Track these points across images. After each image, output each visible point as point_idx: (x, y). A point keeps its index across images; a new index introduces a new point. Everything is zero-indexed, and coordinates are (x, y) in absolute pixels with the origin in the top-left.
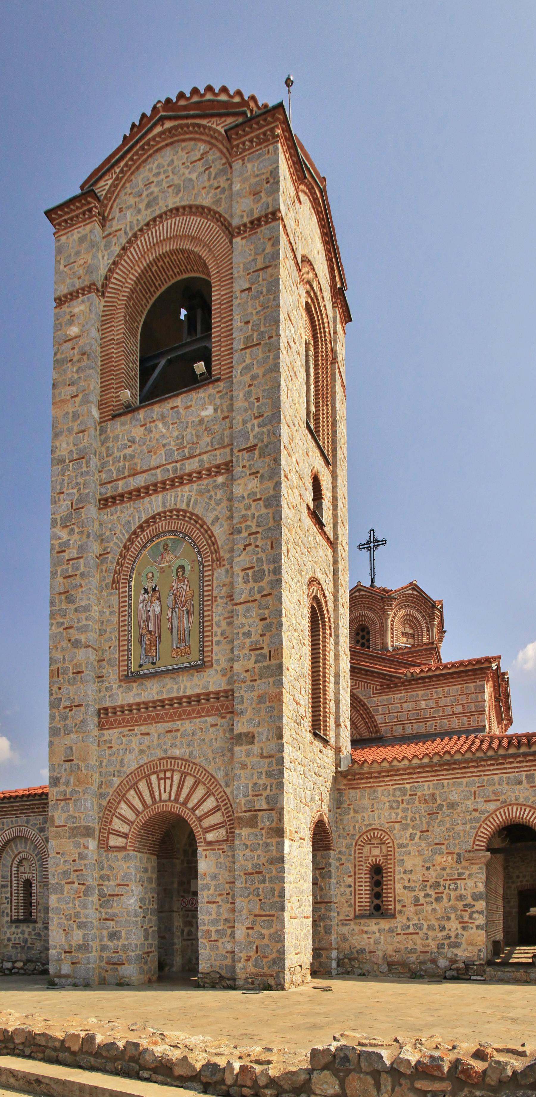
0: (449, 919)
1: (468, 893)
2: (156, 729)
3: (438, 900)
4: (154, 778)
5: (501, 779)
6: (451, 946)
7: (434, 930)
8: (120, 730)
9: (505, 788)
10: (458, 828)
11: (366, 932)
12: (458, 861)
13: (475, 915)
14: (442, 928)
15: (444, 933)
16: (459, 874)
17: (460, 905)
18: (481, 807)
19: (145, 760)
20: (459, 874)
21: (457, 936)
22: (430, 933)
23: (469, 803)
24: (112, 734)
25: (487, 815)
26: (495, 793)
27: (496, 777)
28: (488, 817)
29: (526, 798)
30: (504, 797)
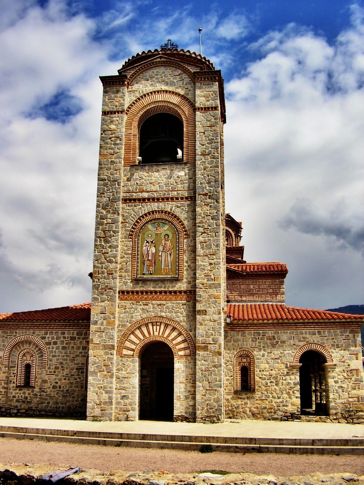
5: (306, 332)
7: (275, 398)
8: (131, 302)
9: (308, 336)
11: (241, 398)
14: (279, 398)
15: (280, 400)
20: (287, 373)
21: (286, 401)
23: (291, 341)
25: (300, 347)
26: (304, 338)
27: (304, 331)
28: (300, 348)
30: (308, 340)
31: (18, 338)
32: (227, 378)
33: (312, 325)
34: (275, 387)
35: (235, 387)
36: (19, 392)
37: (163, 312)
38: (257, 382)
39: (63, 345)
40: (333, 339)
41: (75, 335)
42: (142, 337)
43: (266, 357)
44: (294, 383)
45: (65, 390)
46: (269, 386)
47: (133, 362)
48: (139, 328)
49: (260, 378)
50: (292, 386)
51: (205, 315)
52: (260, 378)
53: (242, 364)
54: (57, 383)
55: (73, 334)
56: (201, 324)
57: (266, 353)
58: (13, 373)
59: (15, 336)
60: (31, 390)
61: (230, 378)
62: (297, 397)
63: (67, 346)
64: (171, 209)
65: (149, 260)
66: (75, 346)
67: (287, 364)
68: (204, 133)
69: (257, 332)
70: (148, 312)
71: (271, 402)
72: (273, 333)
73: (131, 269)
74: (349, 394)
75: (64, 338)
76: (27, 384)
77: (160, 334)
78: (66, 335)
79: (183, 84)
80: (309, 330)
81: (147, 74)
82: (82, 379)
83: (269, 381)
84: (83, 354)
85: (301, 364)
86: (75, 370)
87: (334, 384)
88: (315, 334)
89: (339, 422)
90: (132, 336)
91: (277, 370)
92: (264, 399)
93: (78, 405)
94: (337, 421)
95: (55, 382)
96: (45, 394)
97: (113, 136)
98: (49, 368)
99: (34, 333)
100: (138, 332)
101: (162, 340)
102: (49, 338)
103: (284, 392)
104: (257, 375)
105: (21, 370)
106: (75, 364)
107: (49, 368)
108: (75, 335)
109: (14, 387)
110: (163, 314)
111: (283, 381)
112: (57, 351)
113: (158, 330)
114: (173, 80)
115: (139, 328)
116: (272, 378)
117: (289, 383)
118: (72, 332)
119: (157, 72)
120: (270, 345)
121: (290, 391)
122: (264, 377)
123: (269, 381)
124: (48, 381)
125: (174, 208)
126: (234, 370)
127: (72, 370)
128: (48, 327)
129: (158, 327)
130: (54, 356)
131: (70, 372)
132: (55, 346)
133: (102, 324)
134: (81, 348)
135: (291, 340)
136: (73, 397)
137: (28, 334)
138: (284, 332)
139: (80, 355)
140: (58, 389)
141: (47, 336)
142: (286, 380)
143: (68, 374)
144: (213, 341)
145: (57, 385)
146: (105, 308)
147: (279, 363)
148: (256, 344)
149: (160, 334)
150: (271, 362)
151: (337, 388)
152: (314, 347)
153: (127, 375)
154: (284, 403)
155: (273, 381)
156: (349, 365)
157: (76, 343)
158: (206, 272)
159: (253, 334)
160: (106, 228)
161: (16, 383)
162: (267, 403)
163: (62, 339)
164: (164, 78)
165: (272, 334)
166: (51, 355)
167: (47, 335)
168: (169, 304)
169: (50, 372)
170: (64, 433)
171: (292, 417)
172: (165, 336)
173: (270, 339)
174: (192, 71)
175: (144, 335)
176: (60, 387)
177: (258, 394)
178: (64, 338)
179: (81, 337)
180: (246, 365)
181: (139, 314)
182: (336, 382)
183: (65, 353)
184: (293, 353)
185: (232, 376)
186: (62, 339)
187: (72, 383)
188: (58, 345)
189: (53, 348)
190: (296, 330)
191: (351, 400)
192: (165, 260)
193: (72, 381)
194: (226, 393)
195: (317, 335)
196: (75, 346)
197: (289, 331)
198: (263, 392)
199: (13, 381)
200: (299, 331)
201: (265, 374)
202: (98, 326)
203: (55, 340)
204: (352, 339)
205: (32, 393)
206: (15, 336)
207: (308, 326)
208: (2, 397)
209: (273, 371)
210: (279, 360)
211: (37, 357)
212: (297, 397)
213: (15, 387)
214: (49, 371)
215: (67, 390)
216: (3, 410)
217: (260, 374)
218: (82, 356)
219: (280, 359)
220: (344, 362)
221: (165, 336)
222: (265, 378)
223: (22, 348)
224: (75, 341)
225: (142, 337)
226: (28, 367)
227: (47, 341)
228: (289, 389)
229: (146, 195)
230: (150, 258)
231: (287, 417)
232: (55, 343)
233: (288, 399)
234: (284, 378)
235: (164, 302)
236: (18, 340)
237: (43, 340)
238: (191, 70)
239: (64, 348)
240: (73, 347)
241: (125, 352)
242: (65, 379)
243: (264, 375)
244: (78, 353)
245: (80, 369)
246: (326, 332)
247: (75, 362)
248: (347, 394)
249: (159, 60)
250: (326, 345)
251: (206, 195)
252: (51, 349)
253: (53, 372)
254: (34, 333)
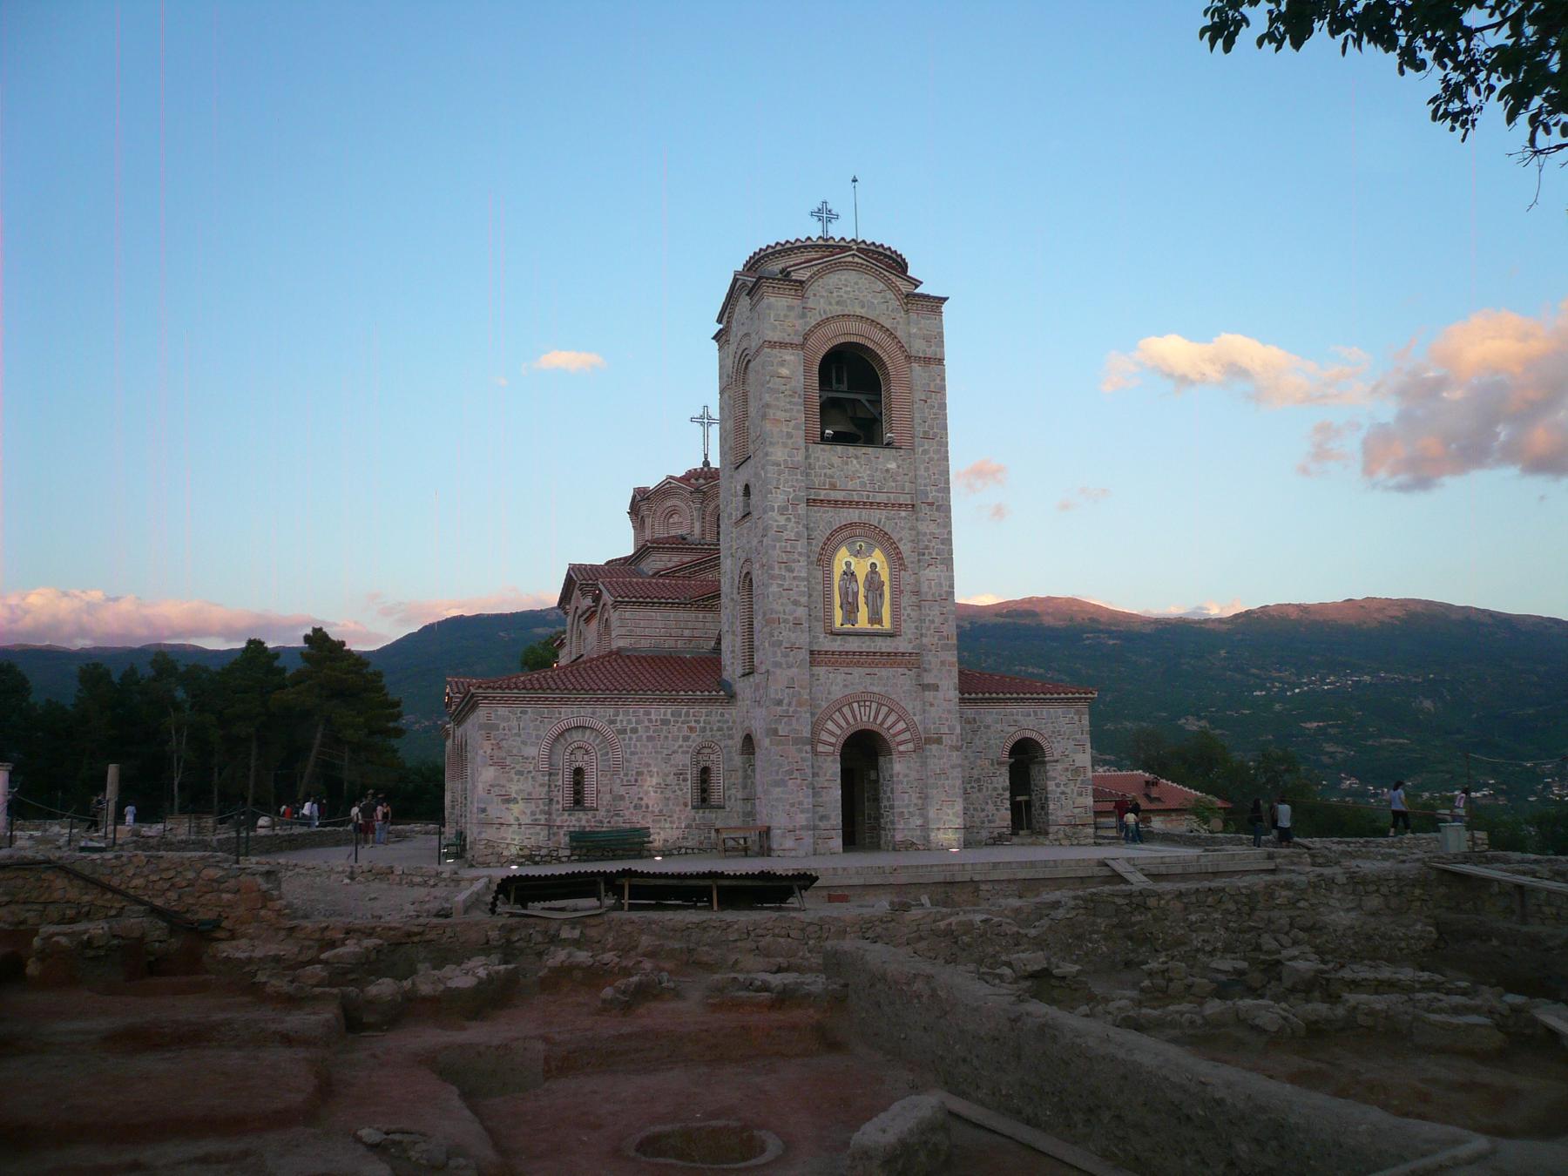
0: (987, 803)
1: (999, 786)
2: (858, 672)
3: (979, 790)
4: (855, 705)
6: (990, 821)
7: (977, 811)
8: (827, 668)
10: (992, 742)
12: (992, 764)
13: (1005, 801)
14: (983, 810)
15: (984, 814)
16: (994, 773)
17: (995, 794)
18: (1007, 729)
19: (848, 691)
21: (993, 815)
22: (975, 813)
23: (998, 726)
24: (820, 671)
26: (1015, 721)
29: (1034, 726)
31: (565, 722)
34: (978, 794)
36: (569, 818)
37: (874, 685)
39: (648, 734)
40: (1052, 723)
41: (669, 716)
42: (843, 724)
45: (657, 810)
47: (834, 761)
48: (839, 710)
50: (1001, 791)
51: (937, 691)
54: (641, 799)
55: (665, 715)
56: (932, 705)
58: (556, 786)
59: (557, 718)
60: (591, 813)
62: (1006, 809)
63: (656, 734)
64: (879, 522)
65: (850, 603)
66: (670, 735)
68: (926, 402)
70: (852, 684)
73: (822, 614)
74: (1074, 803)
75: (650, 721)
76: (578, 801)
77: (871, 720)
78: (653, 717)
79: (888, 309)
81: (831, 281)
82: (685, 790)
84: (685, 749)
85: (1013, 760)
86: (672, 776)
87: (1054, 788)
88: (1030, 715)
89: (1061, 844)
90: (829, 722)
91: (979, 768)
93: (681, 836)
94: (1058, 843)
95: (639, 798)
96: (621, 819)
97: (788, 387)
98: (626, 775)
99: (594, 713)
100: (837, 716)
101: (875, 728)
102: (621, 721)
103: (990, 802)
105: (564, 780)
106: (671, 766)
107: (626, 775)
108: (669, 716)
109: (558, 810)
110: (875, 689)
112: (638, 744)
113: (867, 714)
114: (873, 300)
115: (839, 710)
117: (995, 789)
118: (662, 711)
119: (846, 280)
124: (624, 798)
125: (883, 520)
127: (667, 775)
128: (620, 703)
129: (868, 709)
130: (633, 753)
131: (664, 781)
132: (634, 736)
133: (789, 704)
134: (681, 739)
135: (997, 723)
136: (671, 822)
137: (582, 714)
139: (680, 750)
140: (644, 810)
141: (619, 718)
142: (991, 783)
143: (660, 784)
144: (949, 730)
145: (643, 803)
146: (793, 679)
149: (871, 720)
151: (1058, 795)
152: (1028, 734)
153: (826, 784)
156: (1074, 761)
157: (671, 731)
158: (936, 625)
160: (786, 547)
161: (561, 802)
163: (647, 723)
164: (857, 293)
166: (628, 751)
167: (618, 716)
168: (884, 672)
169: (627, 781)
170: (877, 870)
171: (997, 841)
172: (878, 722)
173: (969, 723)
174: (903, 290)
175: (848, 723)
176: (647, 807)
178: (650, 721)
179: (681, 720)
181: (838, 688)
182: (1058, 785)
183: (653, 747)
186: (647, 723)
187: (668, 799)
188: (640, 734)
189: (630, 739)
191: (1076, 811)
192: (873, 605)
193: (667, 796)
195: (1032, 717)
196: (670, 735)
199: (555, 799)
200: (1008, 710)
202: (784, 708)
203: (634, 725)
204: (1078, 723)
205: (593, 820)
206: (557, 718)
208: (541, 829)
210: (982, 754)
211: (599, 756)
212: (1006, 809)
213: (561, 809)
214: (625, 778)
215: (661, 811)
216: (544, 852)
218: (683, 752)
220: (1067, 756)
221: (878, 722)
223: (569, 739)
224: (670, 727)
225: (843, 724)
226: (579, 772)
227: (619, 727)
229: (839, 496)
230: (850, 600)
231: (994, 838)
232: (634, 731)
233: (995, 812)
235: (876, 670)
236: (563, 725)
237: (612, 726)
238: (901, 287)
239: (650, 738)
240: (666, 737)
241: (821, 748)
242: (656, 792)
244: (676, 748)
245: (681, 774)
246: (1044, 713)
247: (673, 762)
248: (1071, 802)
249: (850, 259)
250: (1044, 731)
251: (931, 504)
252: (627, 742)
253: (633, 780)
254: (594, 713)
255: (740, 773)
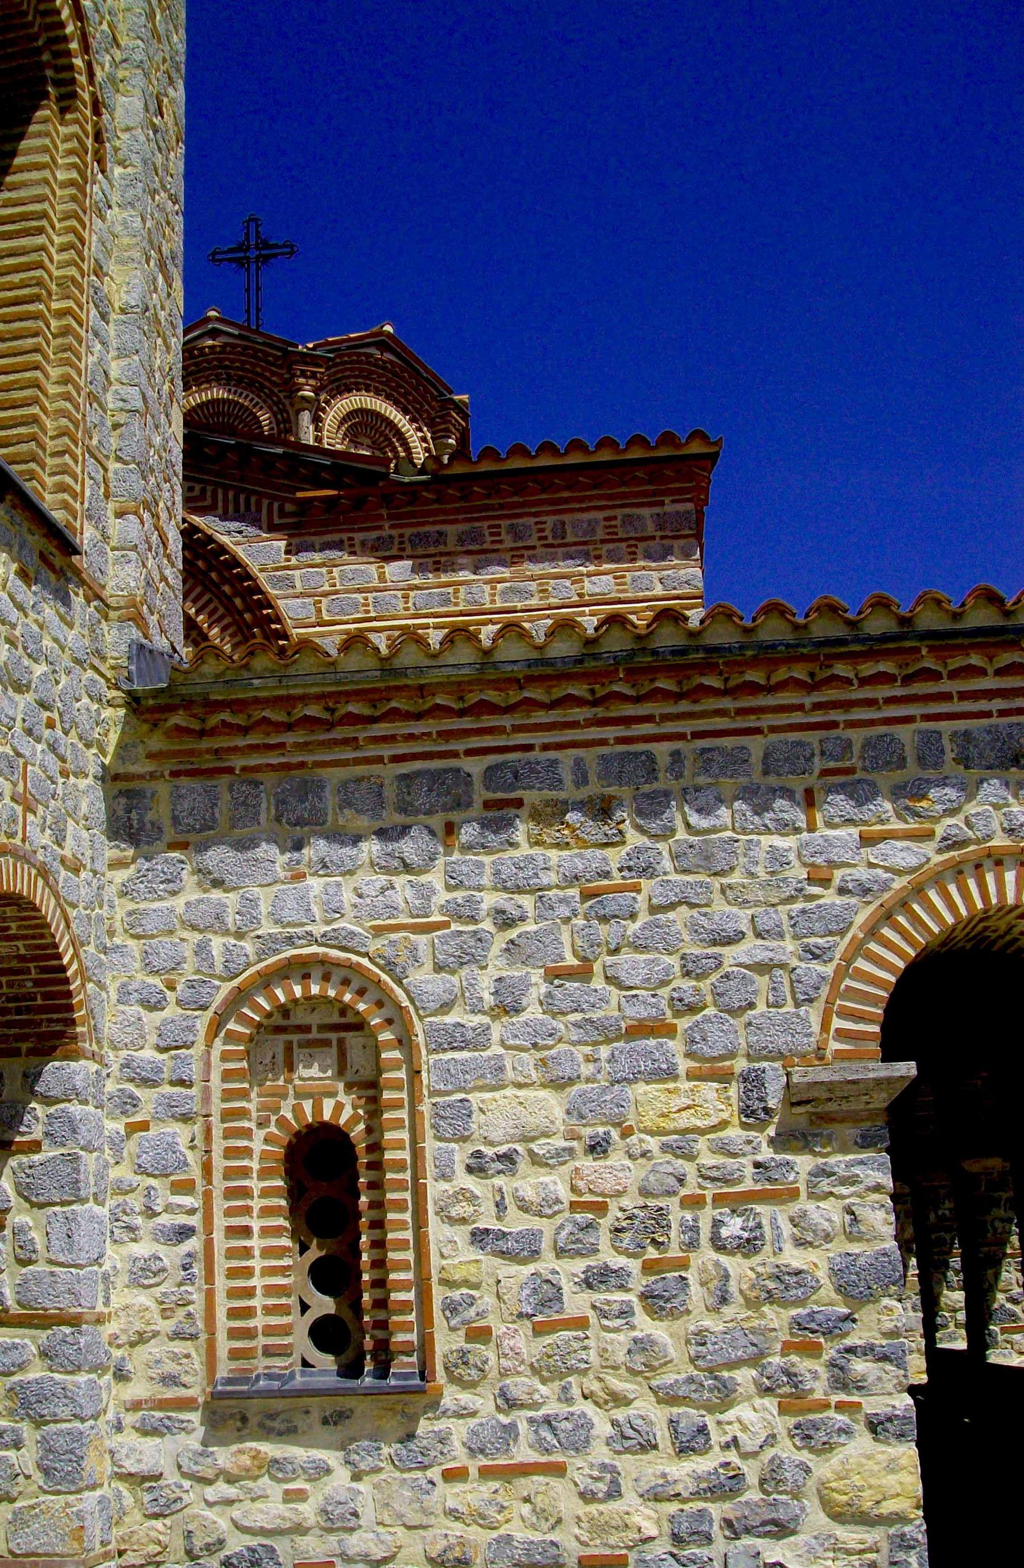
7: (649, 1446)
22: (626, 1464)
27: (904, 733)
32: (142, 1249)
33: (982, 672)
34: (645, 1325)
35: (224, 1345)
38: (447, 1283)
43: (533, 1012)
44: (835, 1272)
46: (582, 1323)
49: (480, 1237)
52: (480, 1237)
53: (297, 1110)
57: (536, 976)
61: (171, 1255)
62: (875, 1426)
67: (752, 1081)
69: (435, 776)
71: (602, 1487)
72: (593, 770)
80: (961, 725)
83: (579, 1266)
85: (908, 1069)
92: (533, 1456)
103: (744, 1376)
104: (442, 1211)
111: (724, 1259)
116: (604, 1239)
120: (574, 892)
121: (803, 1365)
122: (516, 1223)
123: (579, 1266)
126: (207, 1169)
138: (705, 760)
142: (749, 1246)
147: (671, 1074)
148: (426, 893)
150: (587, 1070)
154: (753, 1495)
155: (618, 1261)
159: (390, 792)
162: (569, 1505)
165: (582, 780)
177: (464, 1413)
180: (339, 1107)
184: (814, 954)
185: (185, 1233)
190: (833, 725)
194: (136, 1406)
197: (756, 746)
198: (520, 1385)
200: (858, 736)
201: (529, 1193)
207: (946, 686)
209: (617, 1158)
217: (472, 1198)
219: (683, 1023)
222: (535, 1235)
228: (787, 1348)
233: (786, 1450)
234: (734, 1227)
243: (524, 1207)
255: (494, 1225)
